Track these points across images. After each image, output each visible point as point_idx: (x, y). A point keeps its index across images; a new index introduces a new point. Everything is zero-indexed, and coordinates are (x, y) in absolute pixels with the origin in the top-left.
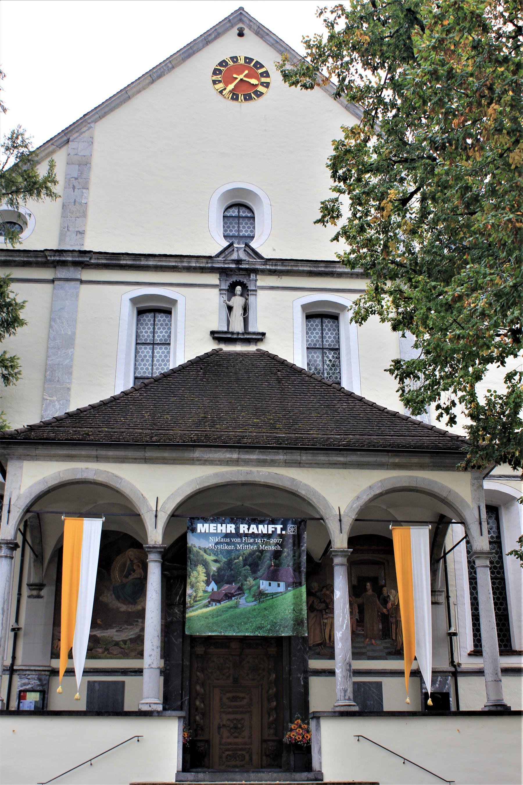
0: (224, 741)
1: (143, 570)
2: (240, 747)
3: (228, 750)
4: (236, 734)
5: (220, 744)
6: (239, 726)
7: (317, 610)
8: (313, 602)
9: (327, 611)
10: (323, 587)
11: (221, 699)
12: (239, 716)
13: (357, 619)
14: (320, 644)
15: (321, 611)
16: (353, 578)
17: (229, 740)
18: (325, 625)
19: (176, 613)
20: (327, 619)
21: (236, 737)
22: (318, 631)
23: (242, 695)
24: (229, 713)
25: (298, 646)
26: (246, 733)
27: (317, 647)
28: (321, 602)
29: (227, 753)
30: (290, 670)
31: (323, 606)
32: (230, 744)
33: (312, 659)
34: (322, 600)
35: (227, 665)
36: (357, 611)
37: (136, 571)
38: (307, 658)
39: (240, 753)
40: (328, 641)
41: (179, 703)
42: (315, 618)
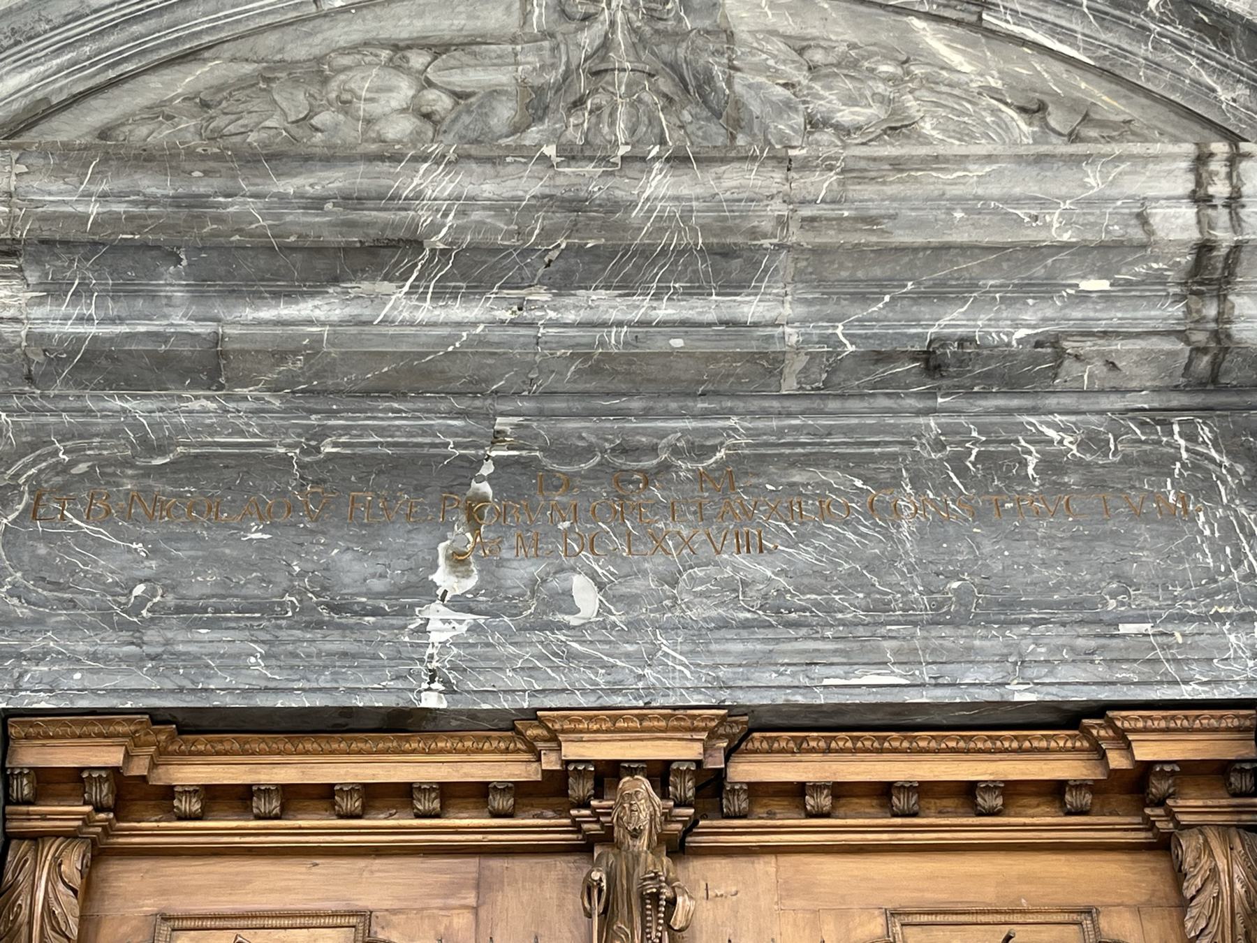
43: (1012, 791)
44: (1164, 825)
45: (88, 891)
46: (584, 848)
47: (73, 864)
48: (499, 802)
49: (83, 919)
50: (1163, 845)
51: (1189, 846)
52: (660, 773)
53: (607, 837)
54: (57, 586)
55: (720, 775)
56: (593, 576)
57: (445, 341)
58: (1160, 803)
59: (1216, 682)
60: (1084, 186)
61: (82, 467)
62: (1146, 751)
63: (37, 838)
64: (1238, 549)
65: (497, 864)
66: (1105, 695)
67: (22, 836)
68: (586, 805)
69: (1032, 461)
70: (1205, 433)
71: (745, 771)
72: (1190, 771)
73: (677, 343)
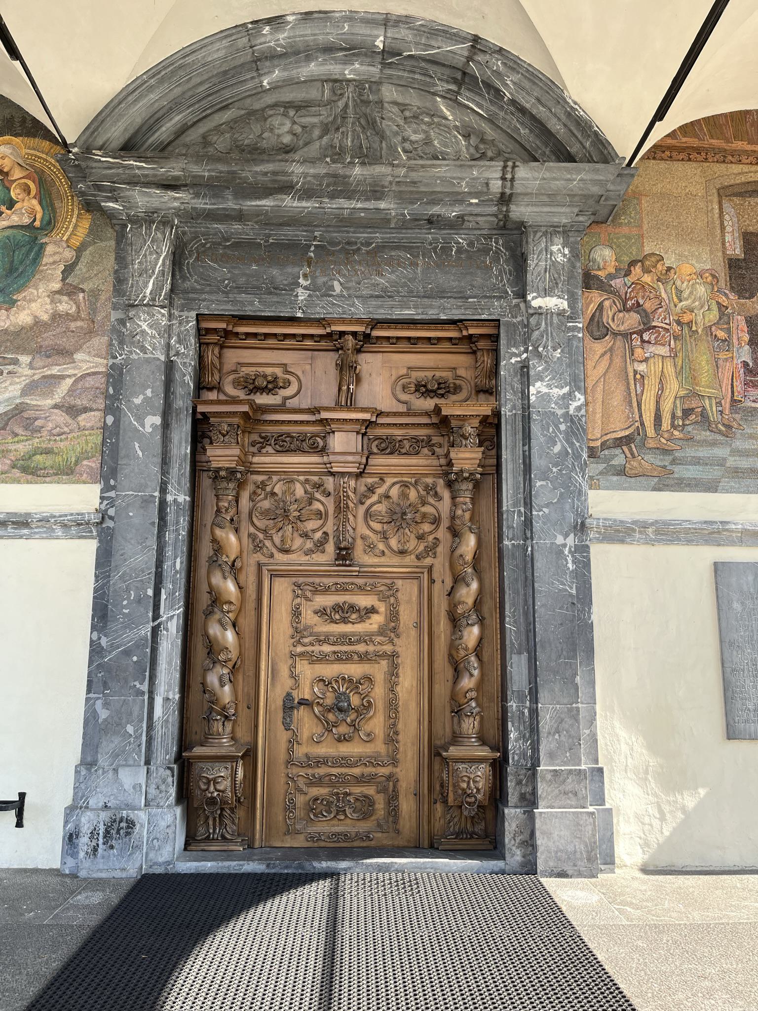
0: (300, 751)
1: (40, 203)
2: (356, 771)
3: (317, 782)
4: (343, 729)
5: (289, 762)
6: (355, 700)
7: (615, 334)
8: (600, 307)
9: (646, 337)
10: (633, 263)
11: (296, 613)
12: (354, 670)
13: (745, 364)
14: (627, 440)
15: (627, 336)
16: (728, 238)
17: (322, 750)
18: (641, 378)
19: (143, 332)
20: (646, 360)
21: (342, 739)
22: (617, 400)
23: (364, 601)
24: (323, 659)
25: (555, 443)
26: (377, 724)
27: (618, 451)
28: (625, 309)
29: (315, 791)
30: (528, 523)
31: (632, 320)
32: (322, 761)
33: (599, 488)
34: (630, 303)
35: (317, 506)
36: (746, 337)
37: (17, 206)
38: (585, 486)
39: (357, 790)
40: (651, 432)
41: (146, 630)
42: (608, 356)
43: (439, 339)
44: (474, 348)
45: (220, 357)
46: (337, 350)
47: (216, 351)
48: (316, 339)
49: (220, 363)
50: (474, 353)
51: (479, 354)
52: (354, 334)
53: (342, 348)
54: (205, 280)
55: (370, 334)
56: (339, 281)
57: (302, 212)
58: (474, 343)
59: (490, 315)
60: (473, 174)
61: (208, 245)
62: (472, 331)
63: (208, 344)
64: (502, 277)
65: (316, 353)
66: (463, 317)
67: (204, 343)
68: (336, 340)
69: (454, 249)
70: (501, 242)
71: (376, 333)
72: (482, 336)
73: (362, 215)
